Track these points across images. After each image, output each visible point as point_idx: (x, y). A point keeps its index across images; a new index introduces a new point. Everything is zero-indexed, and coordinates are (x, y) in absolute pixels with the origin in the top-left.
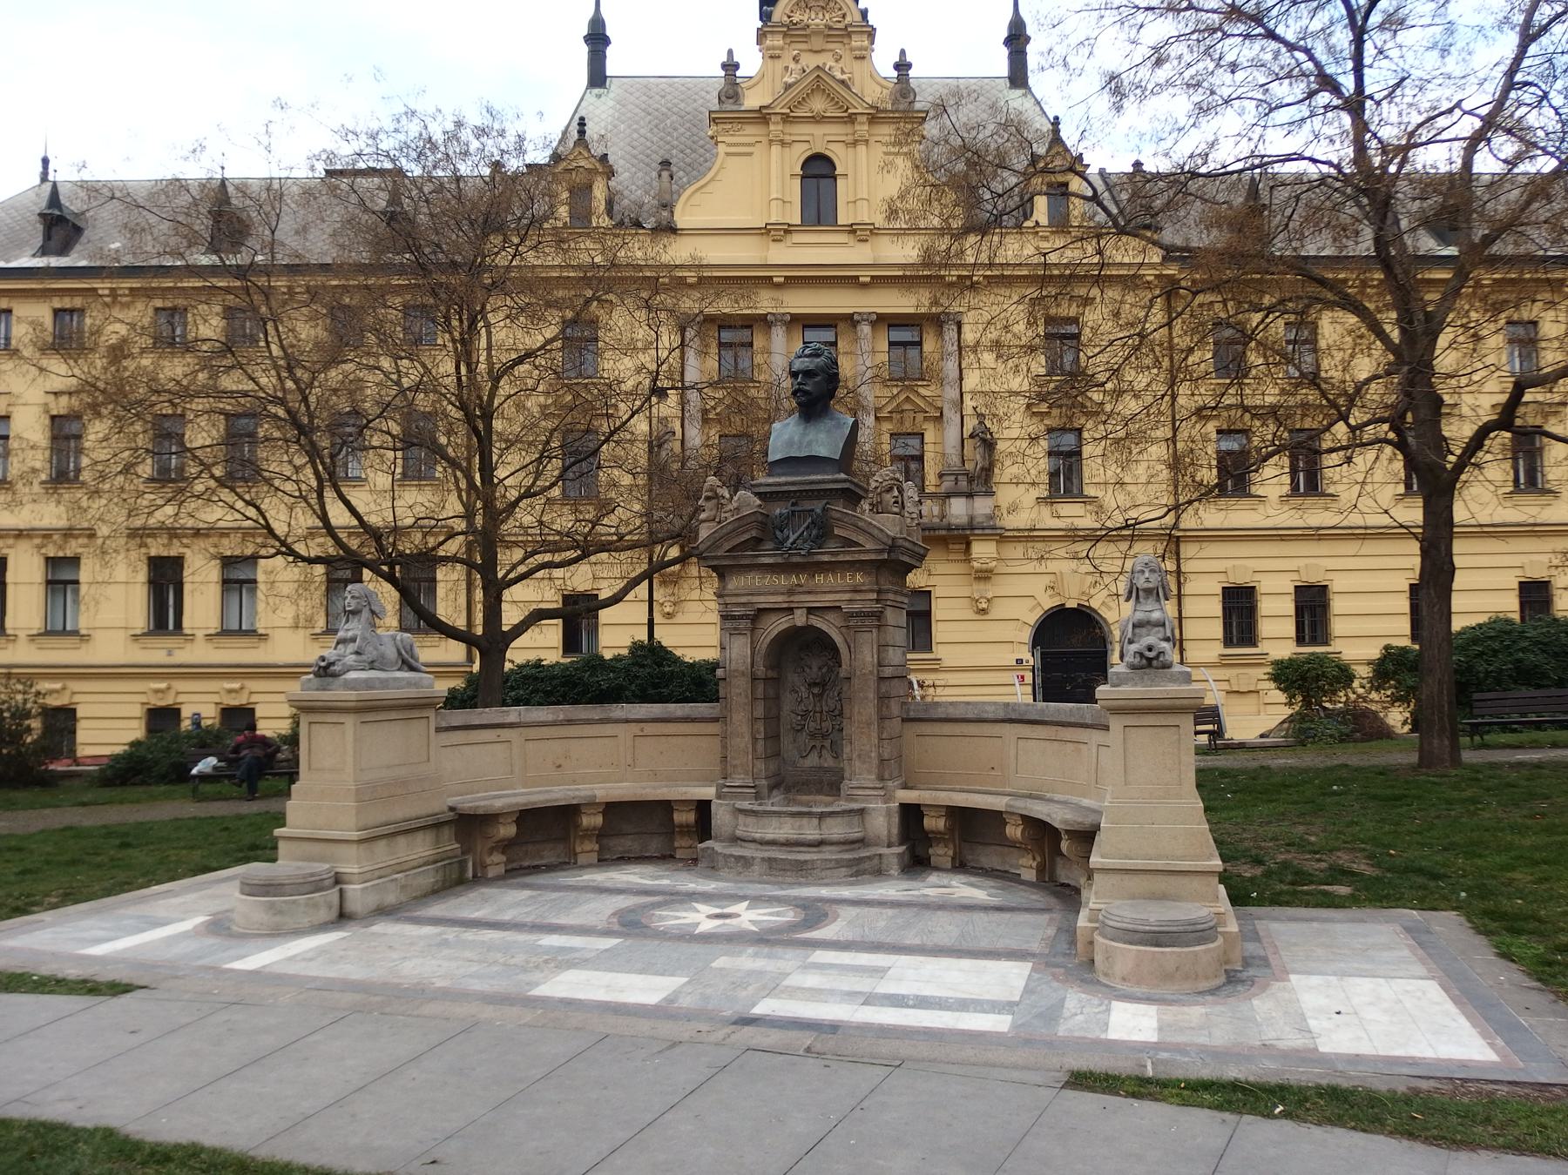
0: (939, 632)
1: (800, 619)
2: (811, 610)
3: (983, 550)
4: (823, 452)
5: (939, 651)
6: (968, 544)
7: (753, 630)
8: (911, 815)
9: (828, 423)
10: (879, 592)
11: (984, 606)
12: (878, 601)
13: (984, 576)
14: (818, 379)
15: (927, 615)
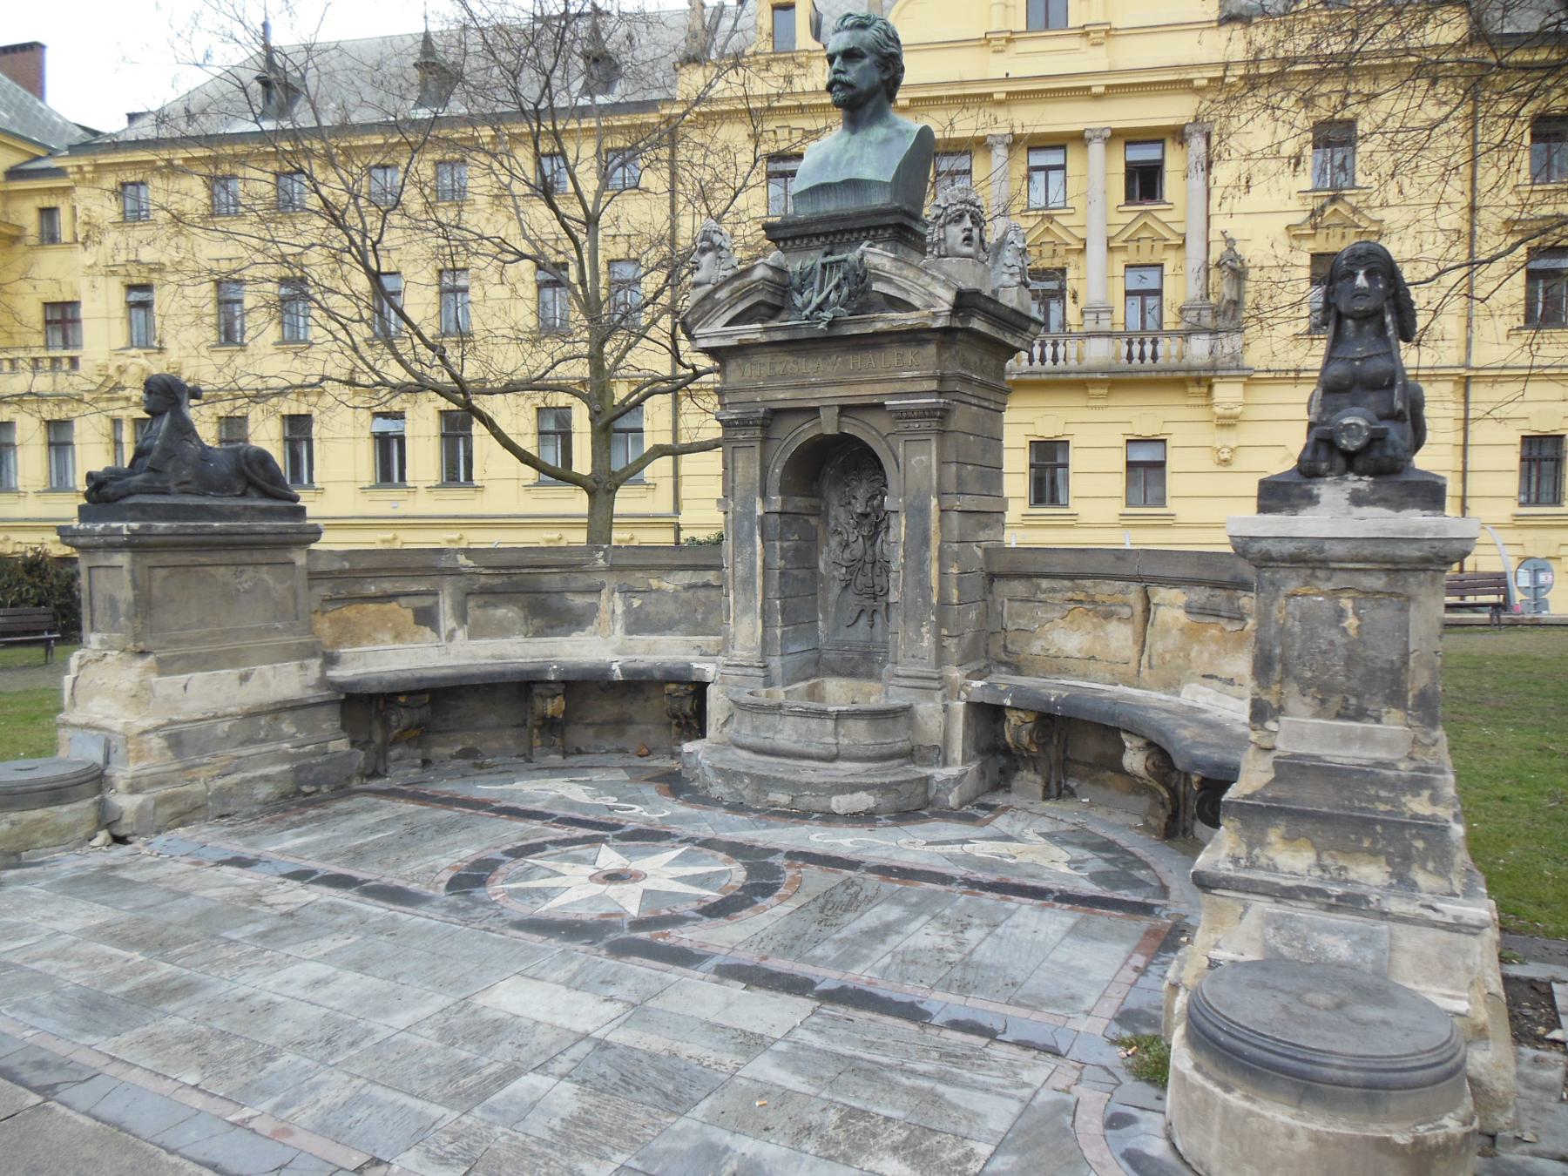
0: (1174, 484)
1: (829, 425)
2: (844, 410)
3: (1227, 394)
4: (867, 173)
5: (1172, 505)
6: (1210, 387)
7: (765, 440)
8: (987, 715)
9: (879, 132)
10: (941, 379)
11: (1226, 456)
12: (940, 393)
13: (1228, 422)
14: (867, 61)
15: (1160, 465)
